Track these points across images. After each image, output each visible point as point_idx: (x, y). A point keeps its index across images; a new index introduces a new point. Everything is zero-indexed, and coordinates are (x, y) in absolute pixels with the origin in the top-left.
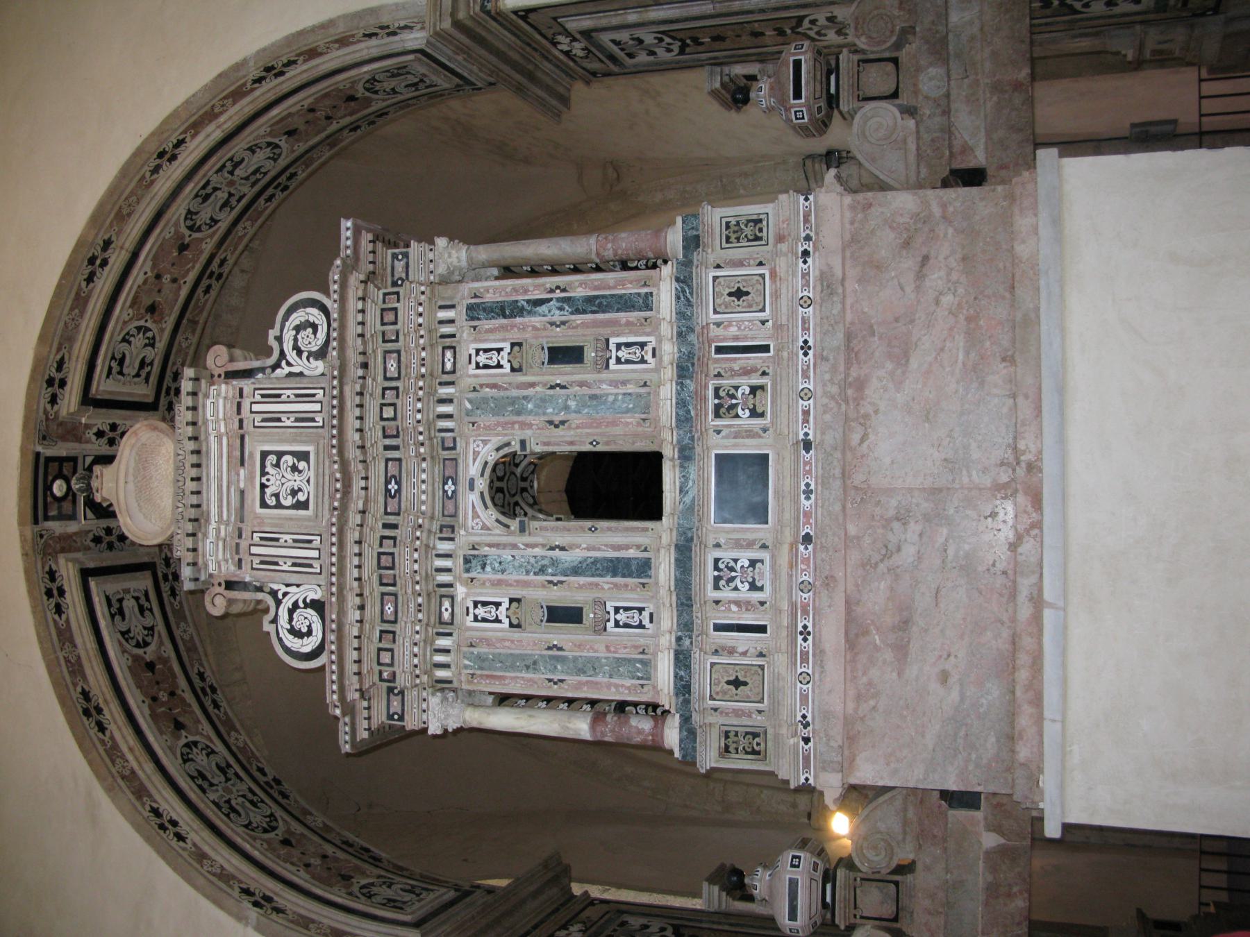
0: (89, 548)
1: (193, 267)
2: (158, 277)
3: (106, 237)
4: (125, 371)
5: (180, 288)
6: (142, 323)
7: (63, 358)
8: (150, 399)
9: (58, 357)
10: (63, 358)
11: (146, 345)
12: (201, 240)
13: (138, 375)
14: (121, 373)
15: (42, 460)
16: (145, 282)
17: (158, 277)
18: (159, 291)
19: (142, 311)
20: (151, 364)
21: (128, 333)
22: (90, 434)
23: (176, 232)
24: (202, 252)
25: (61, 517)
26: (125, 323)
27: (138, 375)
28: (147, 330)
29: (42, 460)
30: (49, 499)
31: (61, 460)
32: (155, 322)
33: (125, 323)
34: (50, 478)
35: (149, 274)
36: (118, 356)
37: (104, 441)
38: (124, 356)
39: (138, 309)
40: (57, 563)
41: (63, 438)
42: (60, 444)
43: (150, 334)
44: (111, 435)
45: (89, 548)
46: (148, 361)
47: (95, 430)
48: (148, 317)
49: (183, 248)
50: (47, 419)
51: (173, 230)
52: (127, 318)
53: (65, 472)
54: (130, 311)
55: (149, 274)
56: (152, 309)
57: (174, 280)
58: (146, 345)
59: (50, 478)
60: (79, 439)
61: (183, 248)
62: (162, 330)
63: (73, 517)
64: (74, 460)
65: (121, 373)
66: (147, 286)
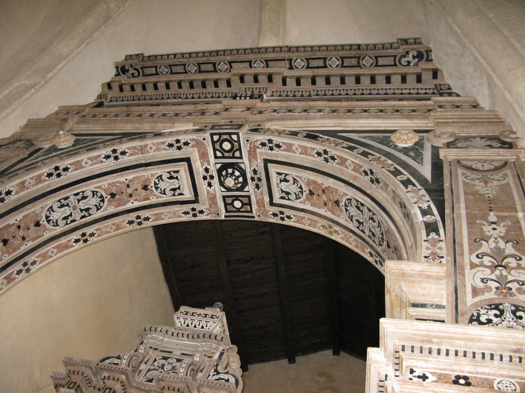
0: (262, 192)
1: (118, 182)
2: (131, 196)
3: (128, 225)
4: (177, 186)
5: (130, 180)
6: (154, 189)
7: (183, 213)
9: (184, 215)
10: (183, 213)
11: (162, 180)
12: (104, 190)
13: (177, 178)
14: (179, 188)
15: (228, 214)
16: (136, 200)
17: (131, 196)
18: (136, 190)
19: (148, 192)
20: (169, 172)
21: (161, 193)
22: (211, 190)
23: (108, 206)
24: (109, 184)
25: (250, 204)
26: (157, 198)
27: (177, 178)
28: (155, 184)
29: (228, 214)
30: (243, 210)
31: (226, 205)
32: (150, 182)
33: (157, 198)
34: (234, 209)
35: (132, 201)
36: (172, 192)
37: (212, 181)
38: (171, 190)
39: (148, 195)
41: (216, 204)
42: (219, 206)
43: (157, 181)
44: (208, 178)
45: (262, 192)
46: (169, 175)
47: (208, 188)
48: (149, 187)
49: (113, 195)
50: (210, 214)
51: (109, 208)
52: (155, 198)
53: (230, 202)
54: (151, 198)
55: (132, 201)
56: (145, 188)
57: (128, 186)
58: (162, 180)
60: (215, 197)
61: (113, 195)
62: (152, 175)
63: (249, 197)
64: (224, 197)
65: (179, 188)
66: (138, 198)
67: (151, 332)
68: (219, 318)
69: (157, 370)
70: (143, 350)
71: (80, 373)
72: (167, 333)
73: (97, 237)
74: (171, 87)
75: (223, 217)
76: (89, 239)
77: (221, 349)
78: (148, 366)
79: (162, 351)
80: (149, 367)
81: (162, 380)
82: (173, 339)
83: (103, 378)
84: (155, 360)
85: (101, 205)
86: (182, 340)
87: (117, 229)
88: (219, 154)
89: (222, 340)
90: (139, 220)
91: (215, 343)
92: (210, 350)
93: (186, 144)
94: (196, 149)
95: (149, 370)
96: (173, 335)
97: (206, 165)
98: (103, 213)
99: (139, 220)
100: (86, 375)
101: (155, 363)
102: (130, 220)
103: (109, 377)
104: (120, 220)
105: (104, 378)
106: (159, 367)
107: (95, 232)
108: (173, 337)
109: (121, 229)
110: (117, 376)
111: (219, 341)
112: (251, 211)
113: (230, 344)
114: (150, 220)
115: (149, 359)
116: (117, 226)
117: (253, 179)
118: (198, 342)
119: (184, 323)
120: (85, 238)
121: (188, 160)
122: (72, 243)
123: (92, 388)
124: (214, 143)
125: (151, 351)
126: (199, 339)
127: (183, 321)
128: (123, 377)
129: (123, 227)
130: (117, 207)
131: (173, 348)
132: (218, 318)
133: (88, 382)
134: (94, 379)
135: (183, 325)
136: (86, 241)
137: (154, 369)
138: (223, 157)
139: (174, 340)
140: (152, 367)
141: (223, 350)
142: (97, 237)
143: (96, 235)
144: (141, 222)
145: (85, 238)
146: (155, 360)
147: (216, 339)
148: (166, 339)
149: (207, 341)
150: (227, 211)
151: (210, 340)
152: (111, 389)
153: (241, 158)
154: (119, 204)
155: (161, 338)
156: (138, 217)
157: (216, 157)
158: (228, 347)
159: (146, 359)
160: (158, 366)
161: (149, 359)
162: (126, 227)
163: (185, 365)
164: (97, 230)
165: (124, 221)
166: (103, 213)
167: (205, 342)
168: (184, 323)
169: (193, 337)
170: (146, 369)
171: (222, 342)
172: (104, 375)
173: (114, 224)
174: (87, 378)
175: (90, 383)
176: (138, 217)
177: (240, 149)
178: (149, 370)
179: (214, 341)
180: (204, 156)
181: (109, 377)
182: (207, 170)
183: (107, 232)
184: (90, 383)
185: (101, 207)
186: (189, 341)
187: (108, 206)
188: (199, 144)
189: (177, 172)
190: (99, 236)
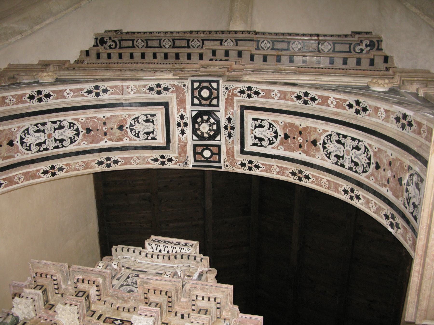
0: (233, 141)
1: (95, 117)
3: (97, 165)
5: (108, 118)
6: (128, 130)
7: (152, 160)
8: (163, 108)
9: (152, 162)
10: (152, 160)
11: (138, 122)
12: (81, 123)
13: (153, 122)
14: (153, 132)
16: (109, 139)
17: (105, 134)
18: (112, 129)
20: (146, 115)
21: (135, 135)
22: (183, 138)
23: (83, 140)
24: (87, 118)
25: (219, 154)
26: (130, 140)
27: (153, 122)
28: (131, 125)
30: (212, 159)
31: (195, 153)
32: (126, 123)
33: (130, 140)
34: (203, 159)
35: (106, 140)
39: (122, 135)
40: (238, 161)
41: (186, 153)
42: (188, 155)
43: (133, 122)
44: (182, 125)
45: (233, 141)
46: (145, 118)
47: (181, 135)
48: (125, 128)
49: (89, 131)
50: (178, 162)
51: (82, 143)
52: (128, 139)
53: (200, 151)
54: (124, 139)
55: (106, 140)
56: (121, 128)
58: (138, 122)
59: (203, 159)
60: (186, 145)
61: (89, 131)
62: (129, 116)
63: (219, 146)
64: (195, 146)
65: (153, 132)
66: (112, 137)
67: (123, 253)
68: (193, 246)
69: (132, 286)
70: (116, 266)
71: (49, 276)
72: (140, 254)
73: (66, 172)
74: (146, 57)
75: (190, 167)
76: (57, 173)
77: (200, 270)
78: (121, 282)
79: (134, 270)
80: (122, 283)
81: (147, 283)
82: (147, 261)
83: (76, 281)
84: (128, 277)
85: (76, 139)
86: (156, 262)
87: (86, 168)
88: (196, 101)
89: (201, 261)
90: (108, 162)
91: (193, 264)
92: (189, 270)
93: (166, 89)
94: (175, 95)
95: (122, 285)
96: (146, 256)
97: (182, 112)
98: (76, 147)
99: (108, 162)
100: (55, 278)
101: (129, 280)
102: (100, 160)
103: (83, 279)
104: (90, 159)
105: (78, 281)
106: (134, 283)
107: (64, 167)
108: (146, 259)
109: (90, 168)
110: (93, 278)
111: (198, 262)
112: (219, 162)
113: (209, 267)
114: (119, 163)
115: (121, 277)
116: (86, 165)
117: (226, 128)
118: (175, 264)
119: (156, 249)
120: (53, 171)
121: (166, 105)
122: (40, 174)
123: (59, 295)
124: (193, 90)
125: (123, 269)
126: (175, 260)
127: (155, 248)
128: (100, 280)
129: (92, 166)
130: (91, 143)
131: (147, 268)
132: (192, 246)
133: (56, 287)
134: (63, 286)
135: (155, 251)
136: (54, 174)
137: (128, 285)
138: (200, 105)
139: (148, 261)
140: (125, 283)
141: (202, 272)
142: (66, 172)
143: (64, 171)
144: (110, 164)
145: (53, 171)
146: (128, 277)
147: (195, 259)
148: (139, 261)
149: (185, 263)
150: (195, 160)
151: (188, 261)
152: (85, 292)
153: (218, 106)
154: (93, 141)
155: (133, 259)
156: (108, 159)
157: (193, 104)
158: (207, 269)
159: (118, 276)
160: (132, 282)
161: (121, 277)
162: (95, 167)
163: (170, 273)
164: (66, 165)
165: (93, 161)
166: (76, 147)
167: (182, 263)
168: (156, 249)
169: (169, 259)
170: (118, 284)
171: (201, 263)
172: (77, 278)
173: (84, 162)
174: (55, 282)
175: (58, 289)
176: (108, 159)
177: (218, 98)
178: (122, 285)
179: (193, 262)
180: (181, 102)
181: (83, 279)
182: (182, 117)
183: (76, 170)
184: (58, 289)
185: (75, 141)
186: (165, 263)
187: (83, 140)
188: (178, 90)
189: (153, 115)
190: (67, 171)
